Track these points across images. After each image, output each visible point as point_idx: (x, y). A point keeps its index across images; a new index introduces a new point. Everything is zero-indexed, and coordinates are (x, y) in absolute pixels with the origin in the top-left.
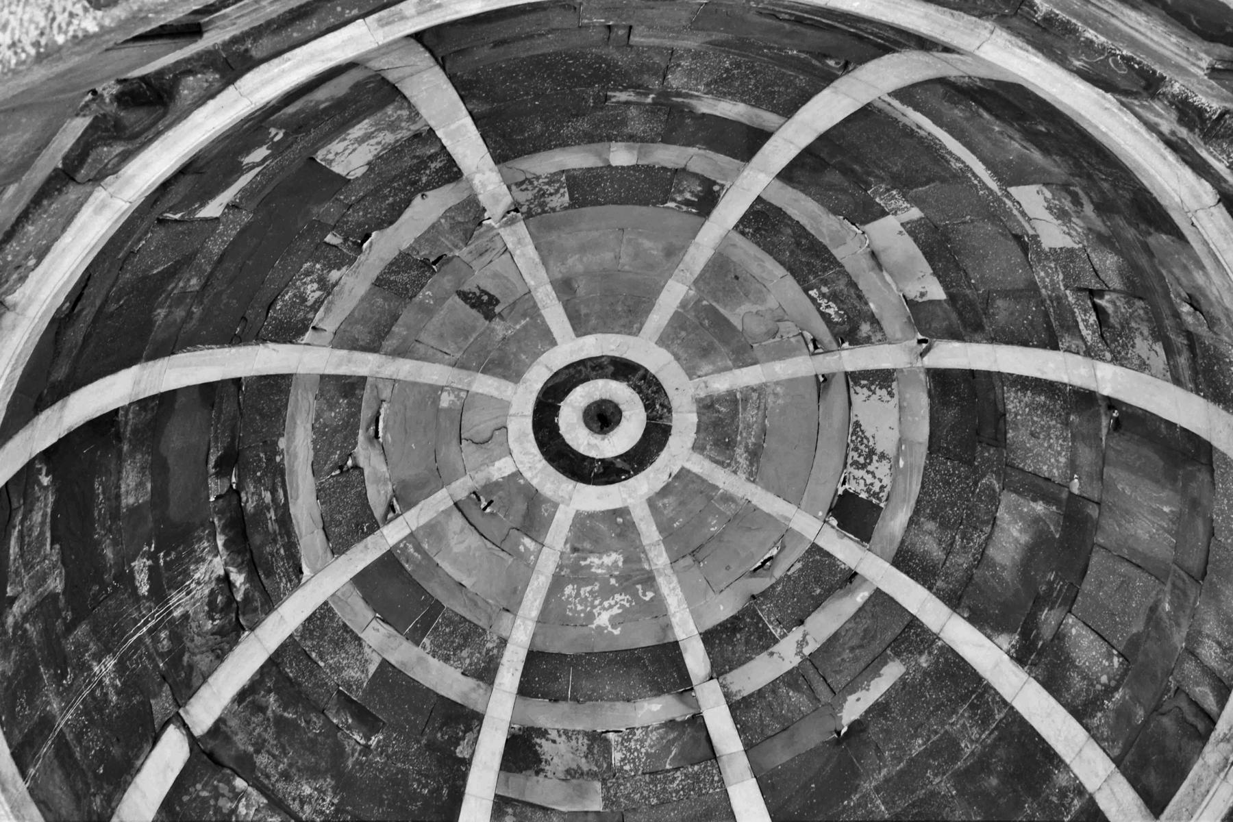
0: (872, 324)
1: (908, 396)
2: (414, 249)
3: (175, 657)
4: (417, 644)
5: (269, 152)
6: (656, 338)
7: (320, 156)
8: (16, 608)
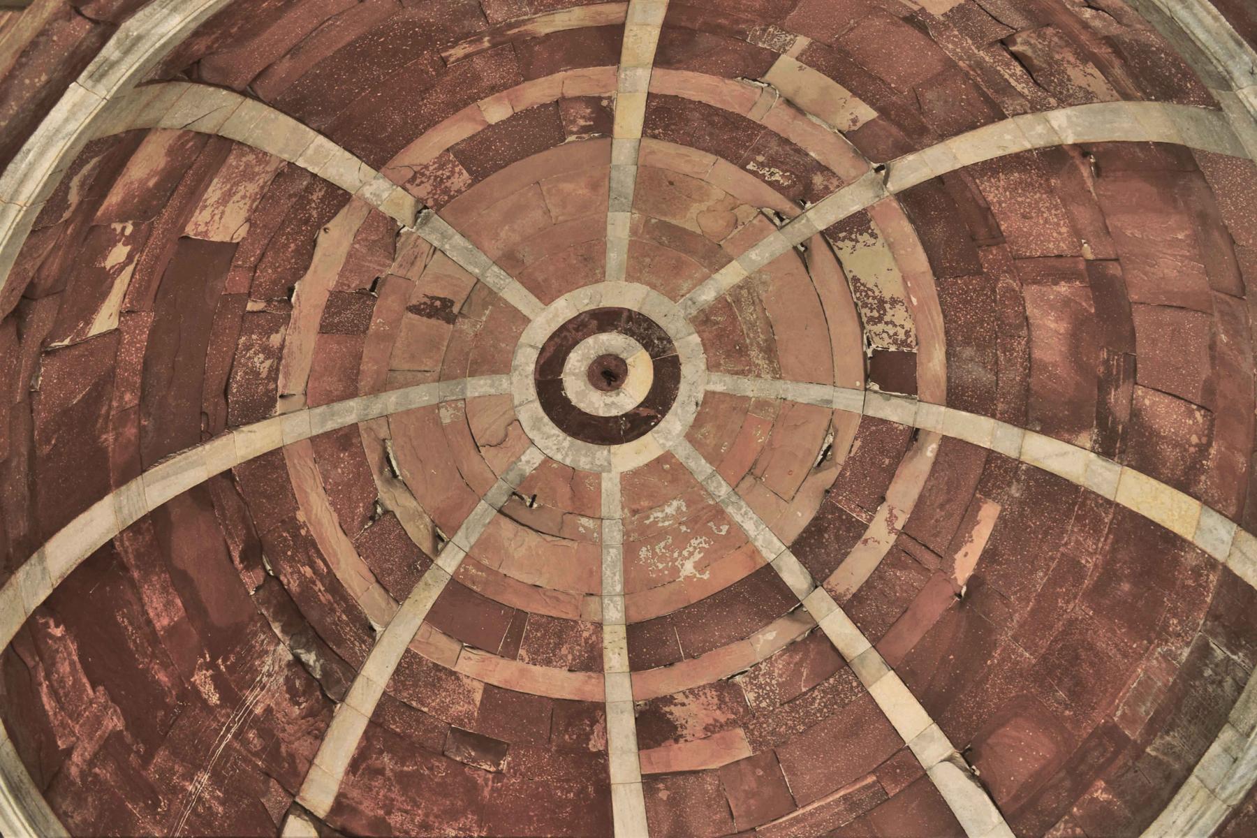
1: (890, 230)
2: (343, 284)
3: (272, 750)
4: (514, 658)
5: (129, 248)
7: (190, 230)
8: (76, 757)
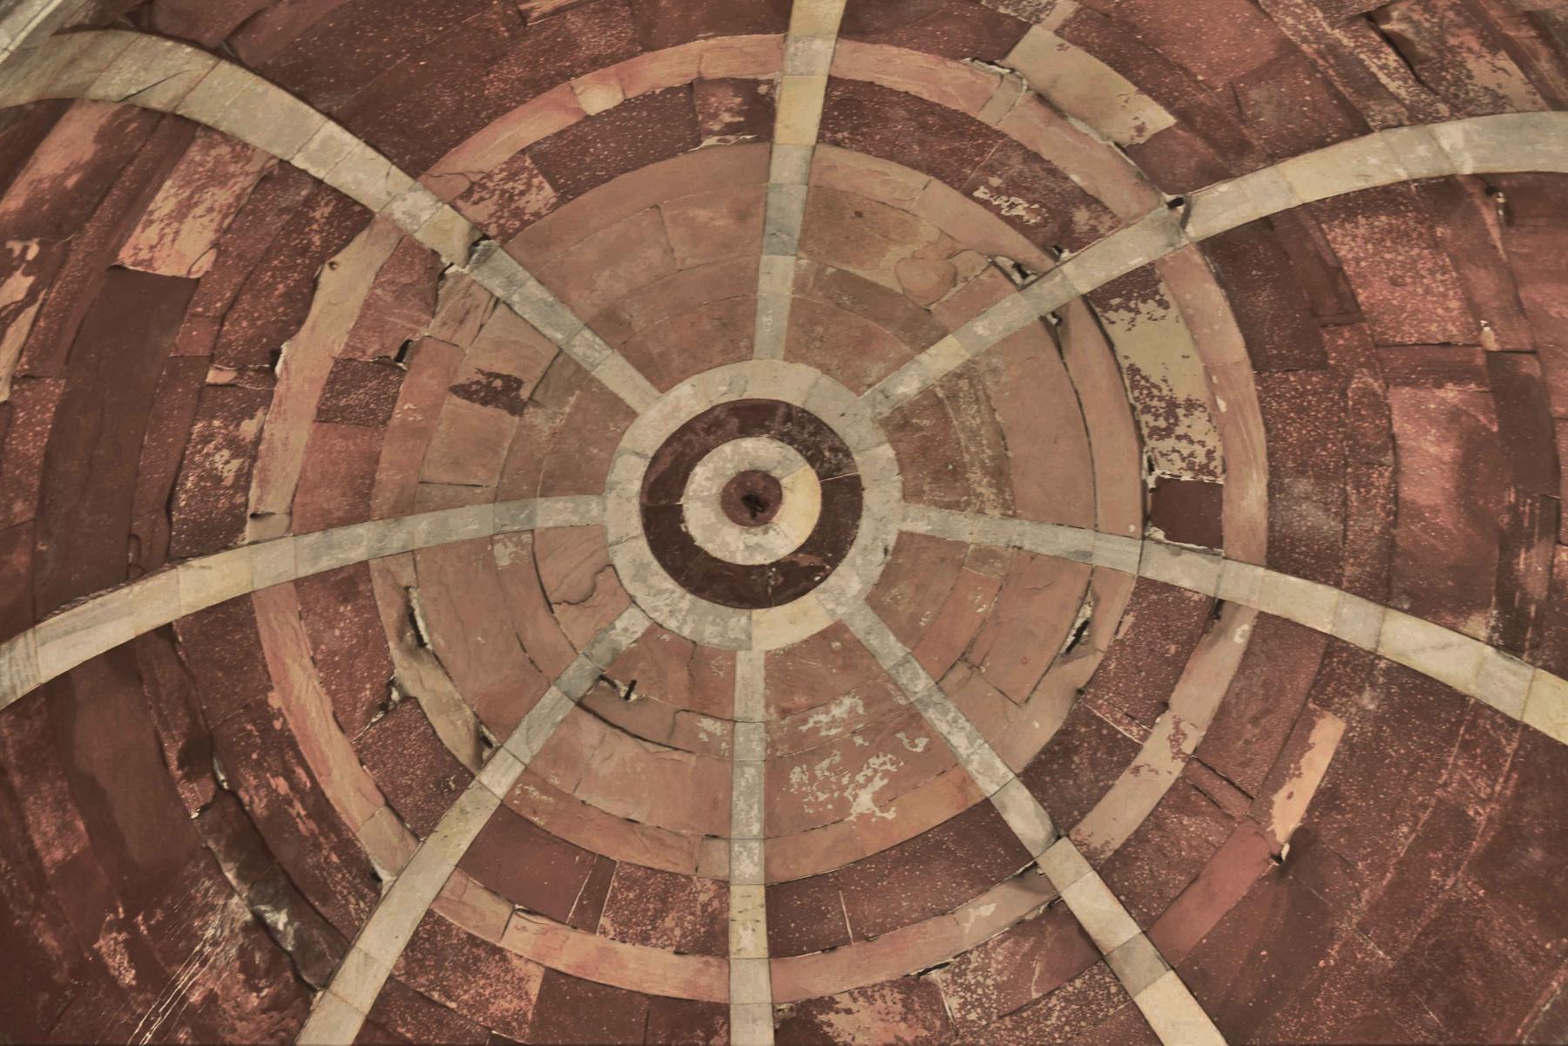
0: (1088, 206)
1: (1188, 296)
2: (354, 348)
4: (592, 929)
5: (31, 279)
6: (781, 353)
7: (126, 257)
